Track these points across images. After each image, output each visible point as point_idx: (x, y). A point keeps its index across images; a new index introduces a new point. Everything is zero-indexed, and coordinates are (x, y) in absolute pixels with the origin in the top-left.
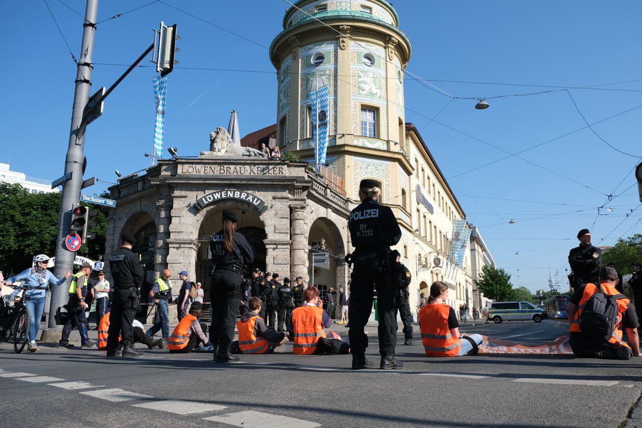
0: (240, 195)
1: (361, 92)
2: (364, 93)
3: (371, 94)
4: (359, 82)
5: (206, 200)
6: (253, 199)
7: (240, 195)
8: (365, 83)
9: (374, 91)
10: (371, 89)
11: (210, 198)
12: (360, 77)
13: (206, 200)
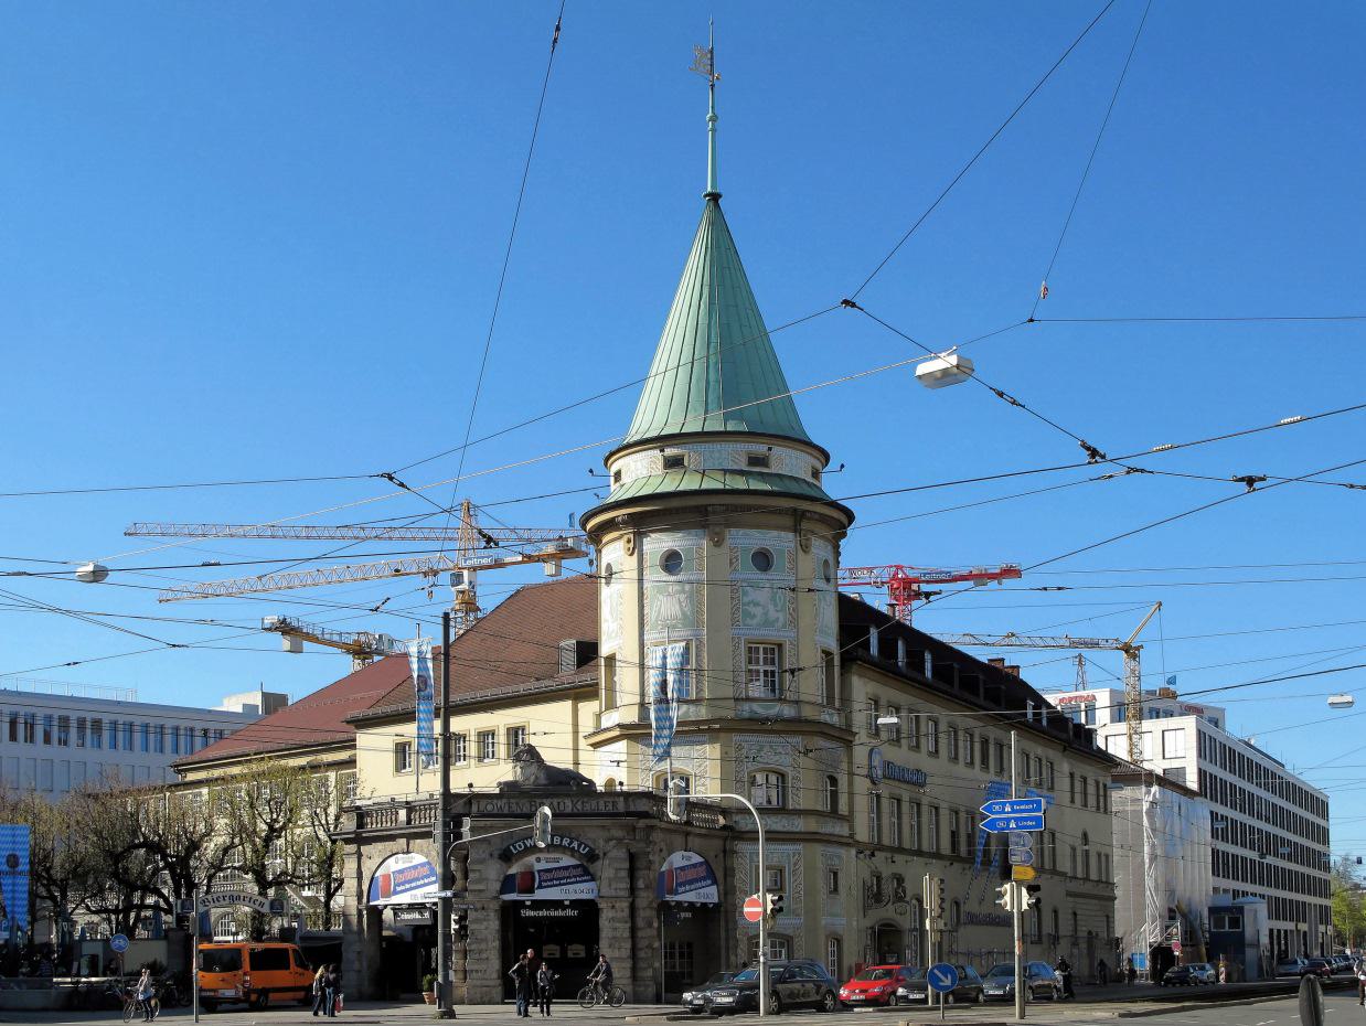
0: (561, 841)
1: (749, 621)
2: (755, 621)
3: (767, 623)
4: (744, 605)
5: (515, 849)
6: (579, 846)
7: (561, 841)
8: (757, 604)
9: (772, 614)
10: (766, 614)
11: (520, 846)
12: (745, 594)
13: (515, 849)
